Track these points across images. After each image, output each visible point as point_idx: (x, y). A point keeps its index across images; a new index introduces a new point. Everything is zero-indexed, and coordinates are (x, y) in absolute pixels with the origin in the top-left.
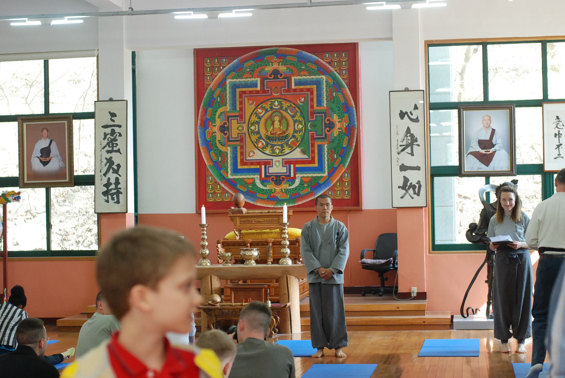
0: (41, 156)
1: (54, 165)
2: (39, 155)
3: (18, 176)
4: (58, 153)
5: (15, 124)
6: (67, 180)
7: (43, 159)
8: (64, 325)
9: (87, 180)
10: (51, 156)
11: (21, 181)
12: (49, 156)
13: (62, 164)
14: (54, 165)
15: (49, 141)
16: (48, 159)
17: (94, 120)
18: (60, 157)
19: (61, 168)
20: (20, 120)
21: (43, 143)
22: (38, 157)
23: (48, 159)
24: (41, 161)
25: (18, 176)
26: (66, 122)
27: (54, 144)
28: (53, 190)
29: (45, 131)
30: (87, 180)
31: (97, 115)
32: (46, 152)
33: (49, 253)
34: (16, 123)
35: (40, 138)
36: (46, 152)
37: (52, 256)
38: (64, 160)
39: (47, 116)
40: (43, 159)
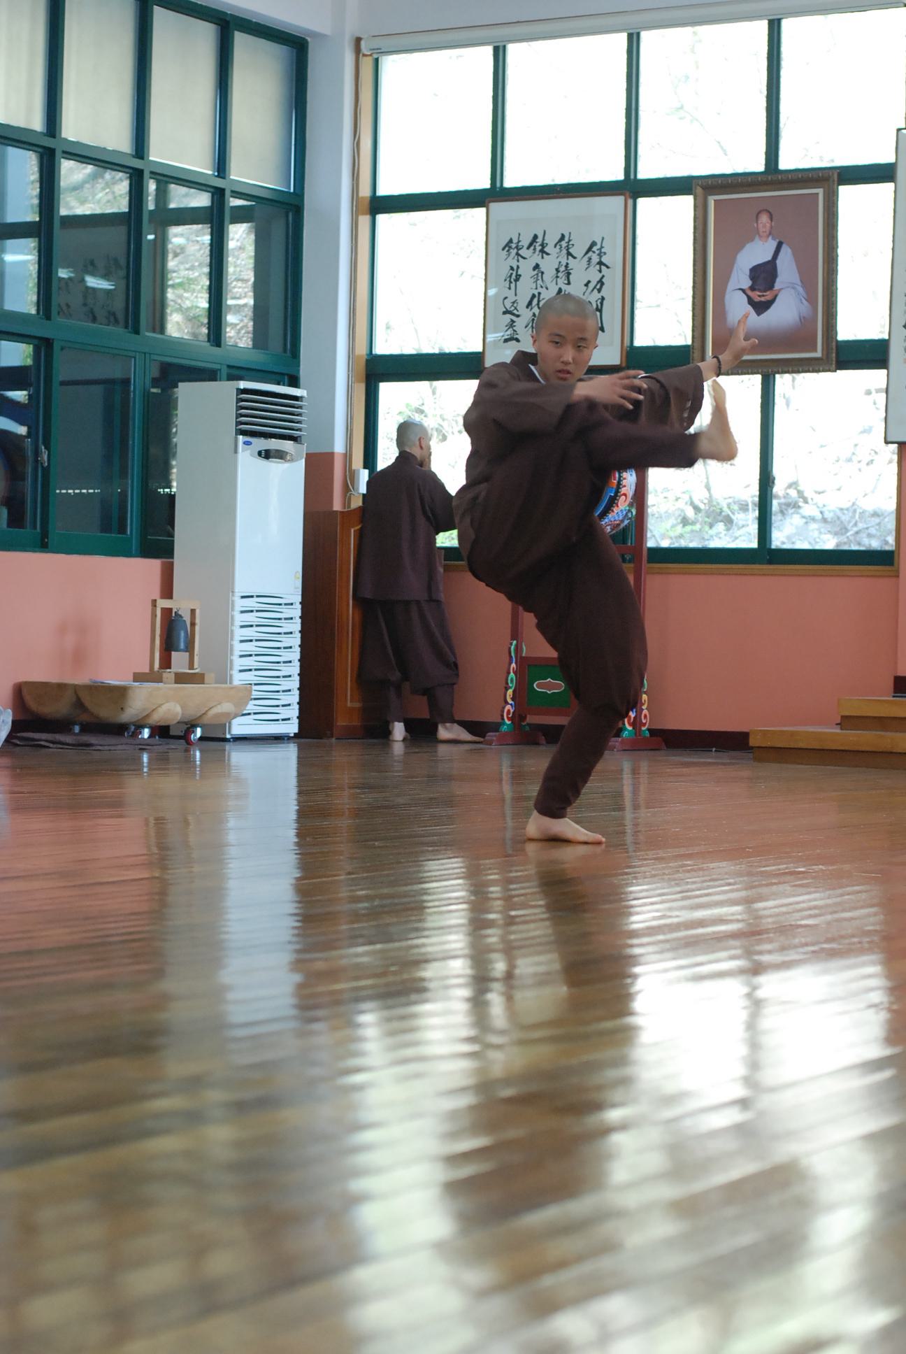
0: (752, 288)
1: (787, 309)
2: (746, 283)
3: (689, 342)
4: (795, 278)
5: (685, 203)
6: (818, 354)
7: (756, 296)
8: (769, 744)
9: (870, 355)
10: (777, 286)
11: (697, 355)
12: (770, 286)
13: (805, 308)
14: (787, 309)
15: (771, 245)
16: (768, 295)
17: (892, 185)
18: (800, 289)
19: (803, 320)
20: (699, 190)
21: (757, 252)
22: (743, 291)
23: (768, 295)
24: (751, 302)
25: (689, 342)
26: (820, 191)
27: (786, 252)
28: (783, 382)
29: (764, 218)
30: (870, 355)
31: (900, 173)
32: (764, 276)
33: (766, 556)
34: (689, 200)
35: (749, 236)
36: (764, 276)
37: (770, 562)
38: (812, 299)
39: (773, 176)
40: (756, 296)
